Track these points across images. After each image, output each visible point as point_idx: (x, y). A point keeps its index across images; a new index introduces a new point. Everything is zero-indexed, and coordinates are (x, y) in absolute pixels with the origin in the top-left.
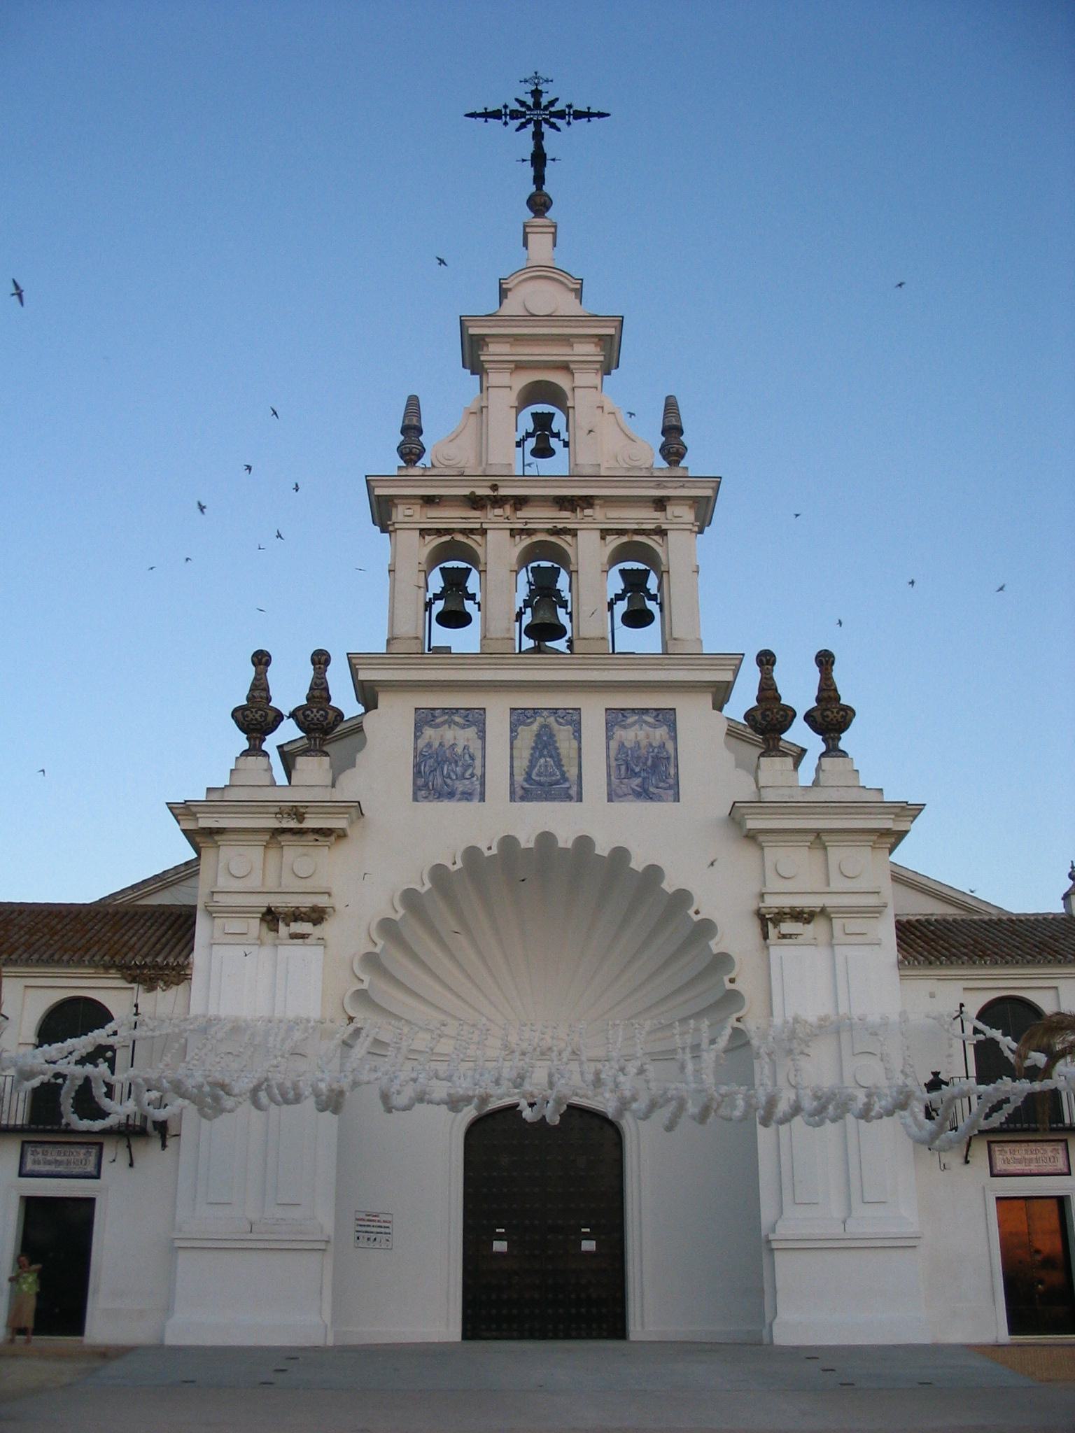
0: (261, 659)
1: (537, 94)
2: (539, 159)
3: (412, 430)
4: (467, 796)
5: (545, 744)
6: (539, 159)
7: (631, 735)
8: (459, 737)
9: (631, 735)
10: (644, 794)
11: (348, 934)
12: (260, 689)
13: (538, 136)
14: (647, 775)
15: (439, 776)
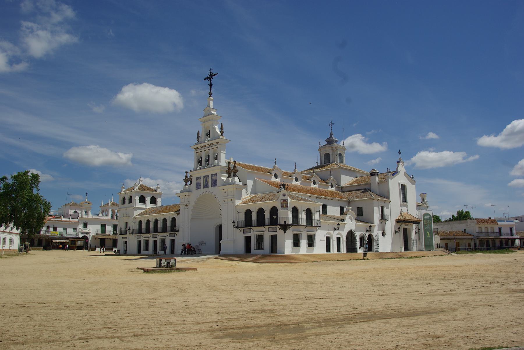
0: (187, 173)
1: (211, 73)
2: (211, 85)
3: (198, 136)
4: (200, 188)
5: (206, 181)
6: (211, 85)
7: (213, 178)
8: (199, 180)
9: (213, 178)
10: (215, 186)
11: (191, 207)
12: (186, 177)
13: (211, 81)
14: (214, 183)
15: (198, 187)
